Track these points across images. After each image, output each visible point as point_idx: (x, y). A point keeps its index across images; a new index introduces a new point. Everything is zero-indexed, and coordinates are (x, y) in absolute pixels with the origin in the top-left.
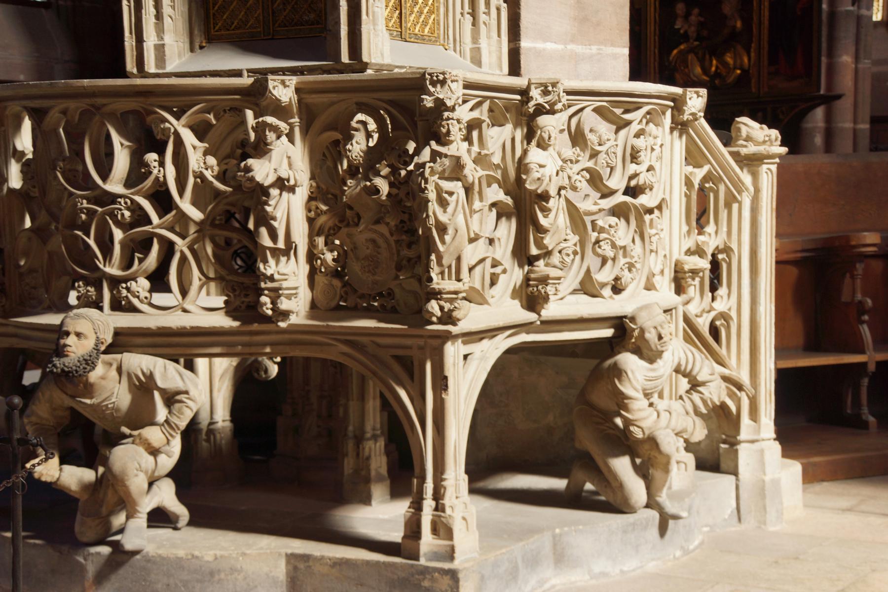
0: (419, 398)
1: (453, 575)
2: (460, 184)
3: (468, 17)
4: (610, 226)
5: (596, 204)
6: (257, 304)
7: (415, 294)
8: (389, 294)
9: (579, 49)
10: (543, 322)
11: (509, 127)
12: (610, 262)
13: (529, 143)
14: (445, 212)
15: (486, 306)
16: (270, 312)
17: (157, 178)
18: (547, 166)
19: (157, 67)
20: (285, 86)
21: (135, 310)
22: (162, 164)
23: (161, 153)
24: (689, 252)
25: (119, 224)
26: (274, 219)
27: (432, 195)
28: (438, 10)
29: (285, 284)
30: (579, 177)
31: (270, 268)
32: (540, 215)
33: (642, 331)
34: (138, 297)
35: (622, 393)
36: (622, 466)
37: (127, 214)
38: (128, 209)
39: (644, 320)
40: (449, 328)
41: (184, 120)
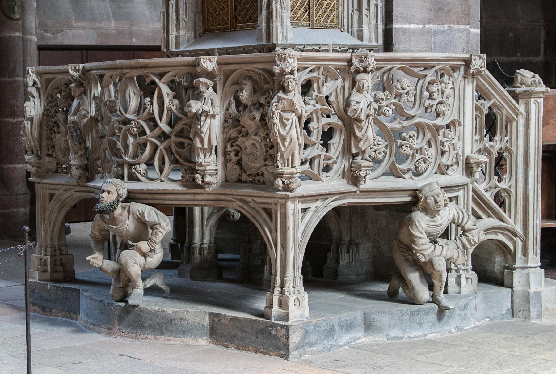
0: (273, 231)
1: (287, 328)
2: (294, 114)
3: (355, 12)
4: (410, 137)
5: (400, 123)
6: (194, 179)
8: (262, 174)
9: (434, 27)
10: (360, 192)
11: (340, 81)
12: (410, 158)
13: (353, 88)
14: (285, 129)
15: (320, 182)
16: (200, 183)
18: (362, 102)
19: (176, 48)
20: (210, 61)
24: (480, 151)
25: (132, 135)
26: (202, 133)
27: (277, 121)
28: (338, 9)
29: (208, 168)
30: (388, 108)
31: (201, 158)
32: (357, 131)
33: (426, 198)
35: (412, 234)
36: (414, 277)
39: (426, 192)
40: (289, 194)
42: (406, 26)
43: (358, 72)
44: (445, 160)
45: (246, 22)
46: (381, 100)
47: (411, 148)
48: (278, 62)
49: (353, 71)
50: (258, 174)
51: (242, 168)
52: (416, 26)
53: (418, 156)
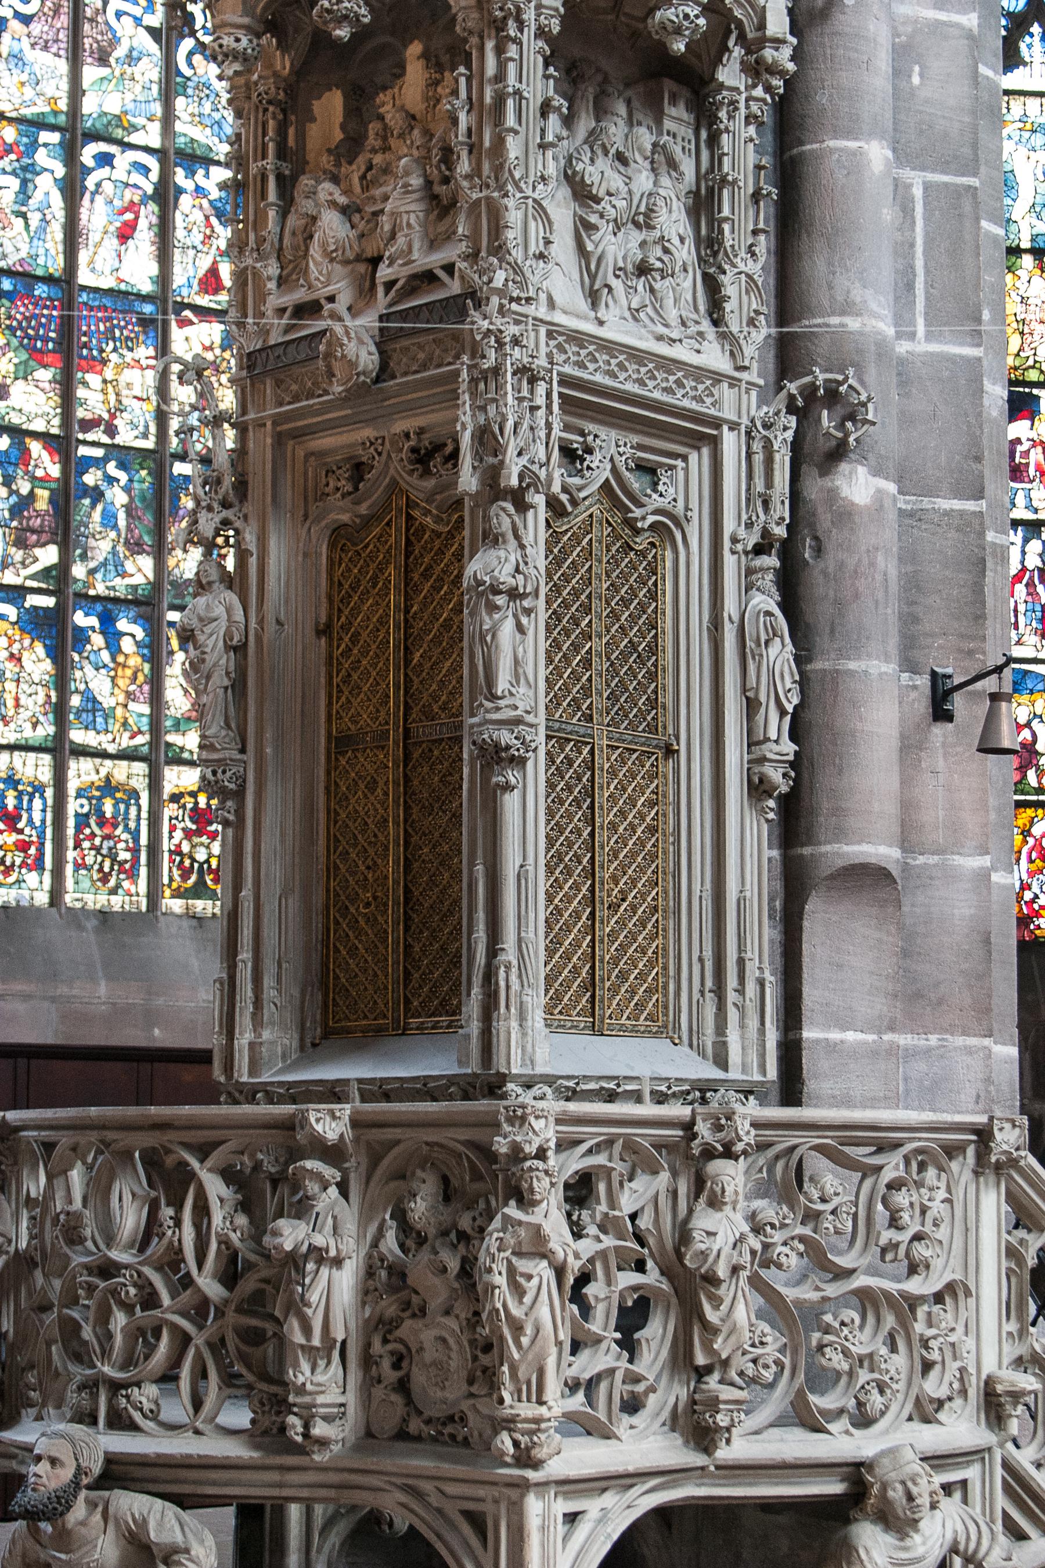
2: (545, 1263)
3: (709, 996)
4: (843, 1324)
5: (817, 1289)
6: (283, 1429)
7: (492, 1419)
8: (462, 1419)
9: (904, 1040)
10: (717, 1467)
11: (665, 1176)
12: (844, 1379)
13: (697, 1197)
14: (521, 1302)
15: (613, 1441)
16: (299, 1439)
17: (171, 1243)
18: (720, 1233)
21: (133, 1427)
22: (178, 1222)
23: (179, 1207)
24: (1019, 1362)
26: (309, 1305)
27: (500, 1280)
28: (665, 987)
29: (320, 1399)
30: (786, 1250)
31: (302, 1374)
32: (707, 1308)
33: (884, 1487)
34: (141, 1410)
37: (132, 1291)
38: (135, 1285)
39: (886, 1470)
40: (531, 1475)
41: (209, 1163)
42: (835, 1035)
43: (709, 1154)
44: (933, 1386)
45: (433, 1015)
46: (768, 1228)
47: (846, 1353)
48: (506, 1128)
49: (696, 1152)
50: (451, 1419)
51: (409, 1401)
52: (860, 1036)
53: (864, 1376)
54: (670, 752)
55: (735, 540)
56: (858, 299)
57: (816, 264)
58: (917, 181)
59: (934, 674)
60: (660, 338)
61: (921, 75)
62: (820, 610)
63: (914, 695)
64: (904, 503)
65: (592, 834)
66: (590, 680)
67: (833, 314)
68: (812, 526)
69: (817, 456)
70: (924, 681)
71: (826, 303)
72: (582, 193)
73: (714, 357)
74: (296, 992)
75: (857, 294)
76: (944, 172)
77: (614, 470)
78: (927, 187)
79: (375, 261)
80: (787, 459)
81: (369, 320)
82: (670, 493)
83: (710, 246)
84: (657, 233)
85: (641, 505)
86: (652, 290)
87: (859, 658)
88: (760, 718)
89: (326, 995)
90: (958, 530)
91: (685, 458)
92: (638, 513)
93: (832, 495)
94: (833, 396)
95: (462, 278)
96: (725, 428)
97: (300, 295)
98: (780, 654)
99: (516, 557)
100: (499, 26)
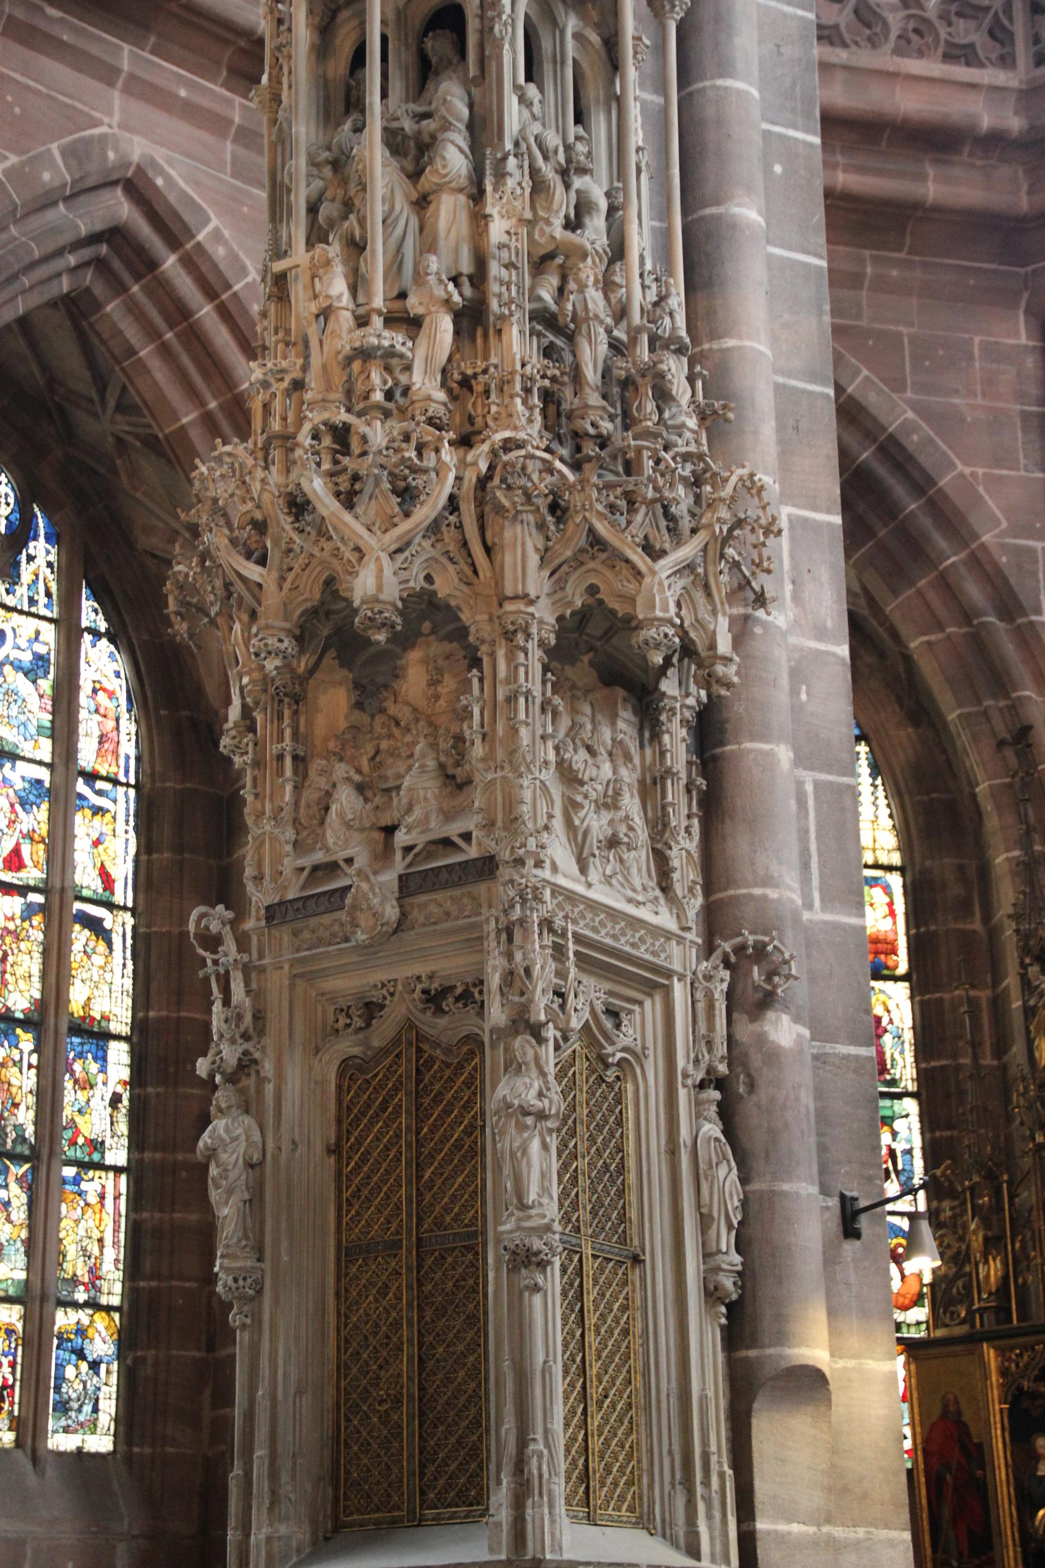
3: (678, 1487)
9: (839, 1532)
45: (450, 1506)
52: (803, 1528)
54: (637, 1260)
55: (686, 1076)
56: (776, 874)
57: (738, 844)
58: (809, 779)
59: (843, 1197)
60: (630, 901)
61: (808, 694)
62: (756, 1140)
63: (827, 1215)
64: (816, 1047)
65: (583, 1335)
66: (577, 1195)
67: (756, 885)
68: (745, 1066)
69: (750, 1002)
70: (834, 1202)
71: (749, 877)
72: (569, 776)
73: (666, 920)
74: (308, 1487)
75: (775, 869)
76: (829, 773)
77: (593, 1012)
78: (817, 784)
79: (390, 830)
80: (724, 1006)
81: (389, 878)
82: (628, 1035)
83: (659, 826)
84: (622, 813)
85: (613, 1043)
86: (622, 861)
87: (790, 1181)
88: (713, 1232)
89: (336, 1489)
90: (855, 1071)
91: (641, 1003)
92: (609, 1049)
93: (761, 1039)
94: (760, 952)
95: (479, 844)
96: (675, 979)
97: (319, 857)
98: (727, 1175)
99: (529, 1084)
100: (509, 636)
